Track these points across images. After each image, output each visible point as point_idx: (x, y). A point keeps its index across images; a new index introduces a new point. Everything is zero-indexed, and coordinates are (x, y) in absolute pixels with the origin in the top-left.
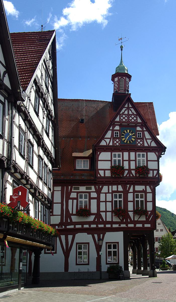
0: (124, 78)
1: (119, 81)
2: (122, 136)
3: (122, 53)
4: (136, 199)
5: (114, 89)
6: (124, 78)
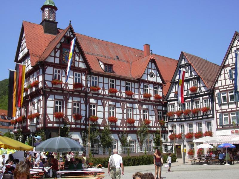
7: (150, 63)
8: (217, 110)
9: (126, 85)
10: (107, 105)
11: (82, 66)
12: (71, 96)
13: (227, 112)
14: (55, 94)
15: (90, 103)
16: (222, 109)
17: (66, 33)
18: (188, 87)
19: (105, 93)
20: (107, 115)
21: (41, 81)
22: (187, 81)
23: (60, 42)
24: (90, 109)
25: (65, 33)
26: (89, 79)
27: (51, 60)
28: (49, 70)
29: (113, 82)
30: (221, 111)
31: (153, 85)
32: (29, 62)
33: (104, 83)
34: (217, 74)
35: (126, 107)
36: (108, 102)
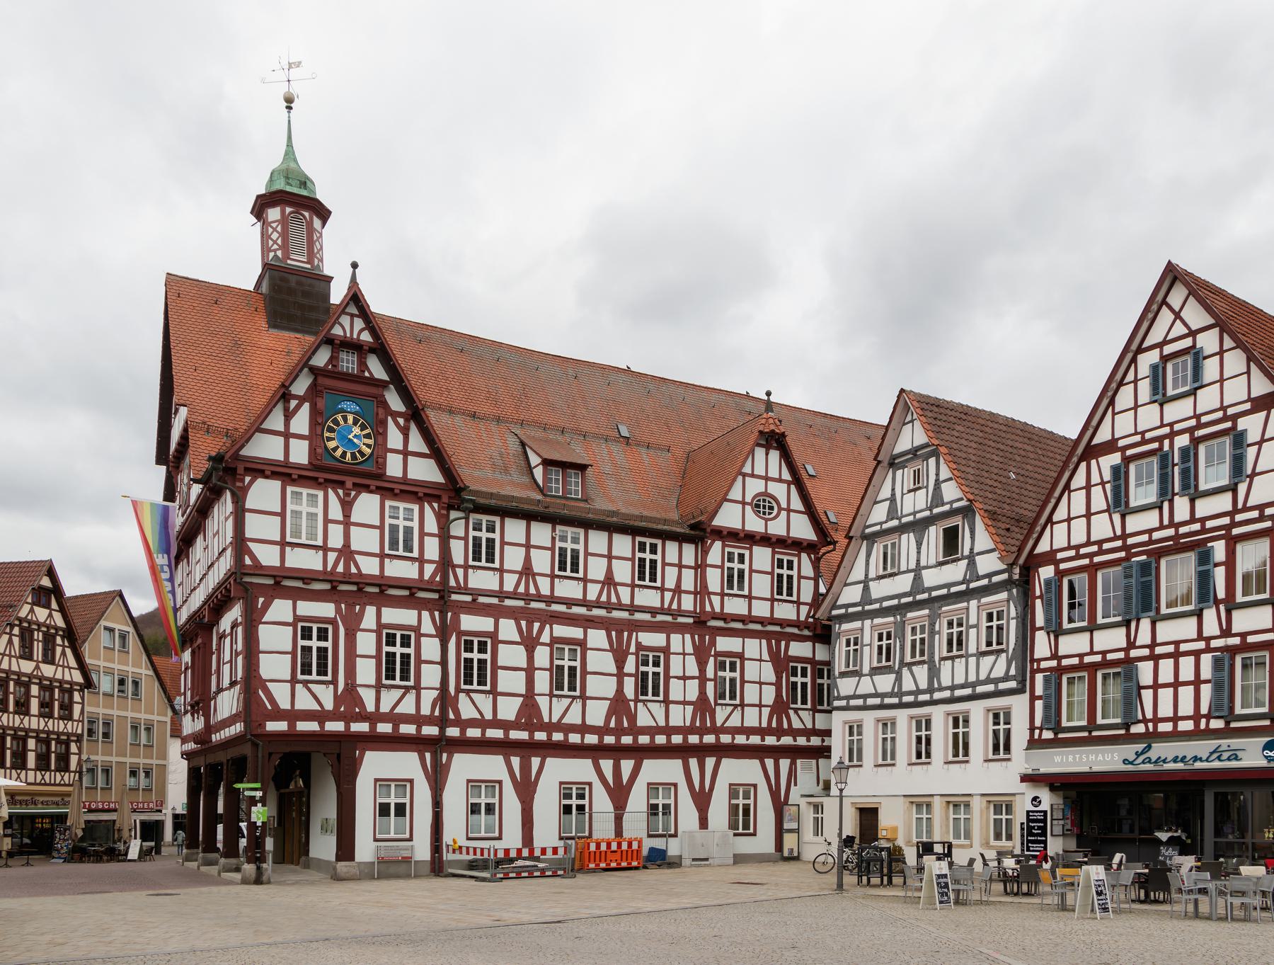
1: (284, 221)
2: (327, 434)
3: (289, 121)
4: (386, 649)
5: (265, 249)
6: (307, 214)
7: (760, 453)
8: (1035, 657)
9: (638, 555)
10: (545, 638)
11: (425, 471)
12: (371, 604)
14: (296, 595)
15: (461, 633)
16: (1060, 654)
18: (919, 553)
19: (532, 591)
22: (918, 526)
24: (465, 655)
26: (457, 529)
29: (491, 529)
30: (1054, 663)
31: (769, 550)
33: (528, 546)
35: (633, 649)
36: (548, 626)
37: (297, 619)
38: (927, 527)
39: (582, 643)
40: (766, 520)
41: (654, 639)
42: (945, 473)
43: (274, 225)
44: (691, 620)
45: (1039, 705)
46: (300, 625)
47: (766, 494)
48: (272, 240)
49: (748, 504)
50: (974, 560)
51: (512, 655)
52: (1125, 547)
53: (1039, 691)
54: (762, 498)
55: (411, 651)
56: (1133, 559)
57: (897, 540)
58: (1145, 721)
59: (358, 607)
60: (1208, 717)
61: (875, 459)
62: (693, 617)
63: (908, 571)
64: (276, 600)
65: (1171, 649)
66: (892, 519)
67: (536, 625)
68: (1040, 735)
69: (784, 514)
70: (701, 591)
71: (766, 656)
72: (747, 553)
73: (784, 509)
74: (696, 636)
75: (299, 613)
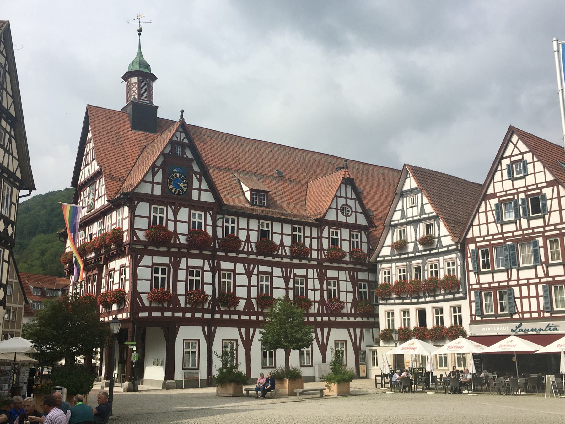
0: (147, 81)
1: (139, 82)
3: (140, 40)
4: (190, 278)
7: (343, 187)
8: (470, 283)
10: (255, 272)
13: (490, 288)
15: (221, 270)
17: (174, 135)
18: (416, 234)
20: (254, 292)
21: (127, 230)
22: (415, 223)
23: (162, 153)
24: (222, 280)
25: (172, 137)
26: (219, 223)
27: (146, 189)
28: (143, 208)
30: (478, 286)
31: (348, 230)
32: (103, 191)
33: (248, 230)
34: (472, 211)
35: (292, 277)
36: (256, 266)
37: (153, 264)
38: (419, 224)
39: (271, 274)
40: (347, 217)
41: (300, 272)
42: (425, 200)
43: (134, 84)
44: (316, 263)
45: (473, 304)
46: (155, 267)
47: (346, 205)
48: (133, 91)
49: (339, 209)
50: (440, 239)
51: (242, 280)
52: (503, 238)
53: (473, 298)
54: (344, 207)
55: (200, 278)
56: (507, 243)
57: (405, 228)
58: (518, 313)
59: (178, 259)
60: (543, 311)
61: (395, 192)
62: (317, 261)
63: (412, 242)
64: (145, 256)
65: (525, 282)
66: (403, 219)
67: (252, 266)
68: (475, 318)
69: (354, 213)
70: (320, 249)
71: (348, 279)
72: (339, 231)
73: (354, 212)
74: (319, 270)
75: (154, 262)
